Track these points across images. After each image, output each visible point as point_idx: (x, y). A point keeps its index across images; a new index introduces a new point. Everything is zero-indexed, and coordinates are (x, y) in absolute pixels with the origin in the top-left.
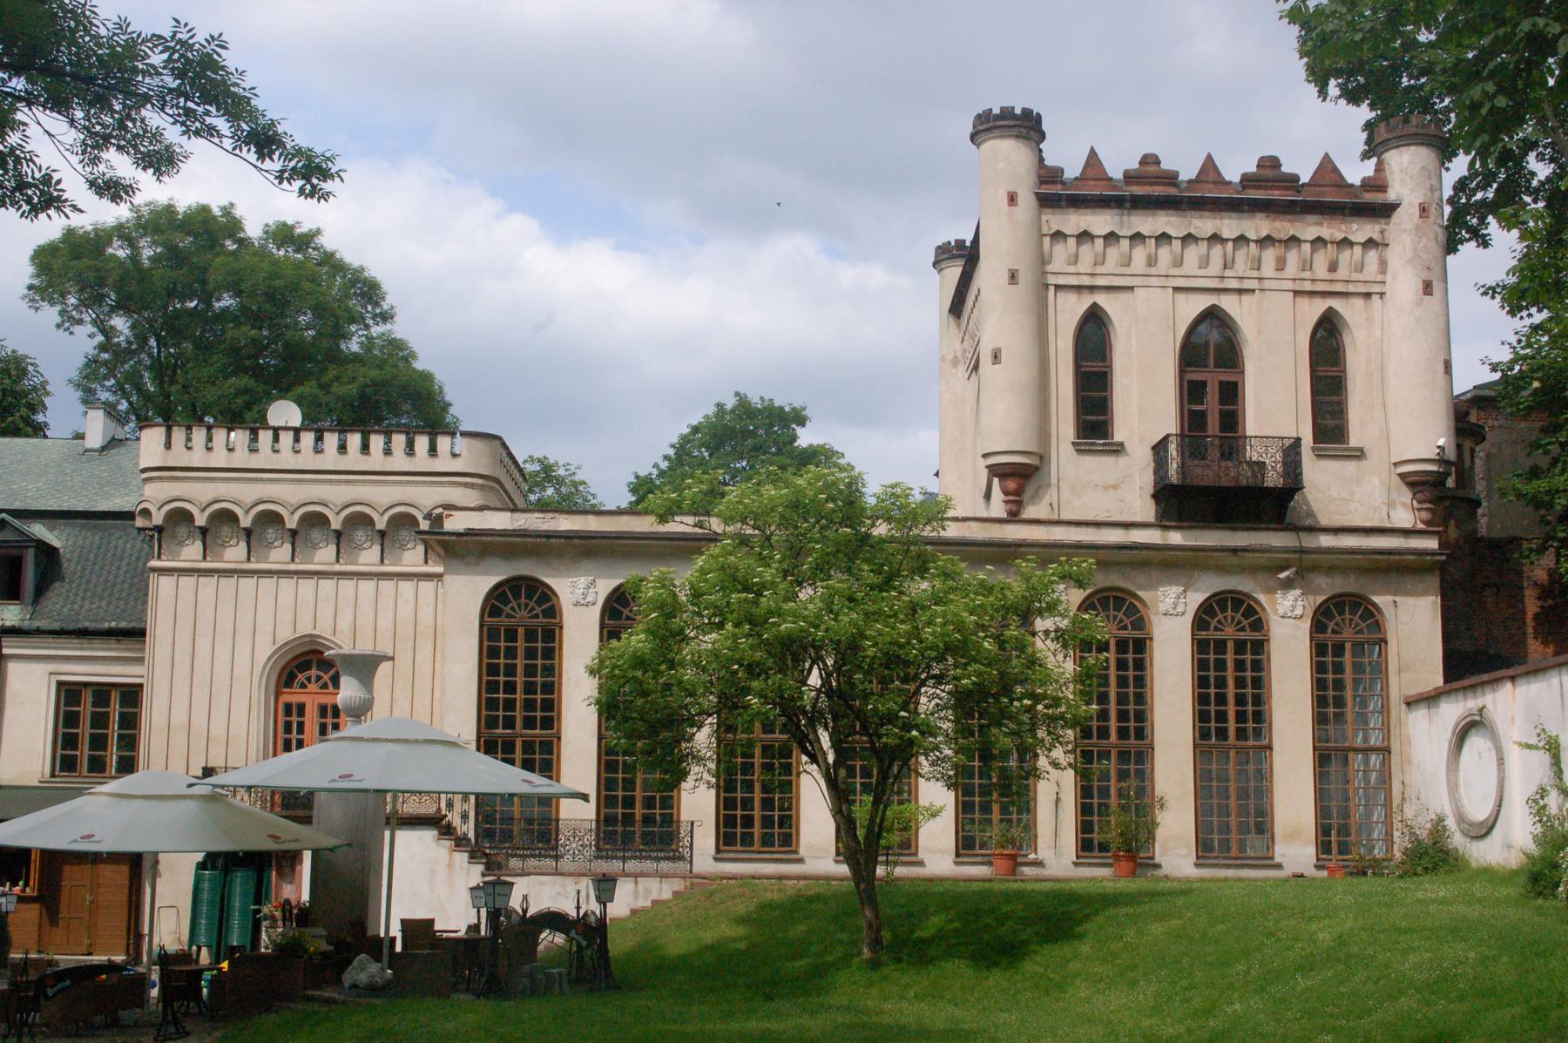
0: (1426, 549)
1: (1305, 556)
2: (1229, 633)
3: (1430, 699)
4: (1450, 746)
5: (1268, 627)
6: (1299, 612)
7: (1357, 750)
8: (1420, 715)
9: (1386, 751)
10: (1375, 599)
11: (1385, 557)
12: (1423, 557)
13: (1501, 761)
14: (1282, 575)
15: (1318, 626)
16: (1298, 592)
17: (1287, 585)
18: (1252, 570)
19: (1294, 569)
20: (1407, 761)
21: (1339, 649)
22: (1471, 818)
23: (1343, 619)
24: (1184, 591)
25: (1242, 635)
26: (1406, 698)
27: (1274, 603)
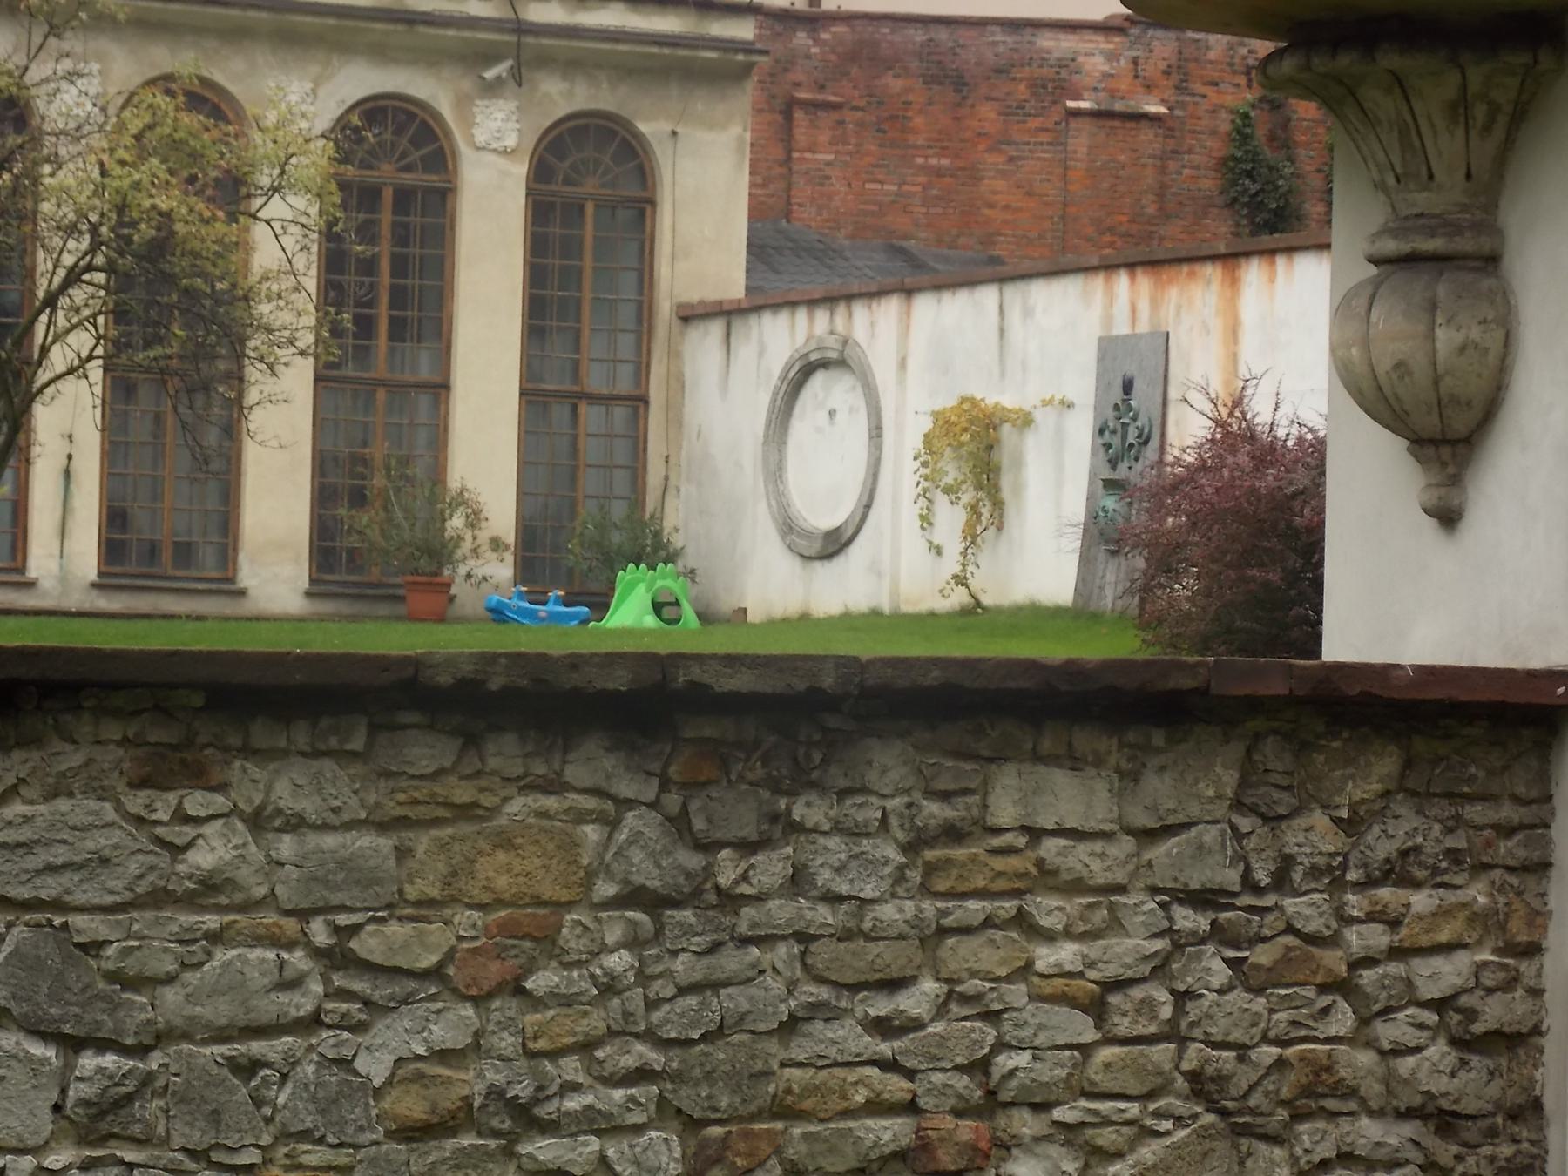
0: (732, 41)
1: (530, 40)
2: (386, 173)
3: (728, 313)
4: (774, 401)
5: (455, 167)
6: (511, 141)
7: (593, 398)
8: (704, 343)
9: (640, 401)
10: (643, 127)
11: (666, 51)
12: (730, 56)
13: (876, 432)
14: (490, 74)
15: (541, 172)
16: (512, 105)
17: (492, 89)
18: (430, 58)
19: (508, 63)
20: (675, 420)
21: (574, 211)
22: (804, 525)
23: (393, 144)
24: (314, 91)
25: (409, 178)
26: (680, 306)
27: (468, 123)
